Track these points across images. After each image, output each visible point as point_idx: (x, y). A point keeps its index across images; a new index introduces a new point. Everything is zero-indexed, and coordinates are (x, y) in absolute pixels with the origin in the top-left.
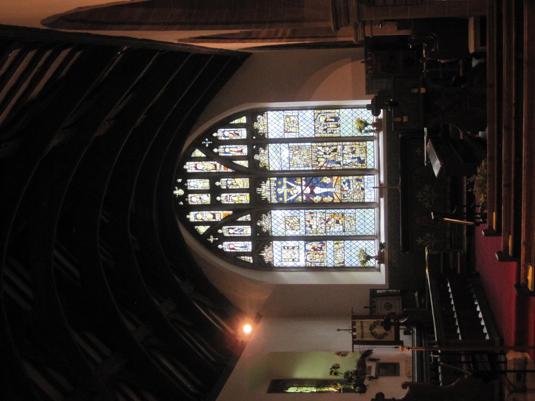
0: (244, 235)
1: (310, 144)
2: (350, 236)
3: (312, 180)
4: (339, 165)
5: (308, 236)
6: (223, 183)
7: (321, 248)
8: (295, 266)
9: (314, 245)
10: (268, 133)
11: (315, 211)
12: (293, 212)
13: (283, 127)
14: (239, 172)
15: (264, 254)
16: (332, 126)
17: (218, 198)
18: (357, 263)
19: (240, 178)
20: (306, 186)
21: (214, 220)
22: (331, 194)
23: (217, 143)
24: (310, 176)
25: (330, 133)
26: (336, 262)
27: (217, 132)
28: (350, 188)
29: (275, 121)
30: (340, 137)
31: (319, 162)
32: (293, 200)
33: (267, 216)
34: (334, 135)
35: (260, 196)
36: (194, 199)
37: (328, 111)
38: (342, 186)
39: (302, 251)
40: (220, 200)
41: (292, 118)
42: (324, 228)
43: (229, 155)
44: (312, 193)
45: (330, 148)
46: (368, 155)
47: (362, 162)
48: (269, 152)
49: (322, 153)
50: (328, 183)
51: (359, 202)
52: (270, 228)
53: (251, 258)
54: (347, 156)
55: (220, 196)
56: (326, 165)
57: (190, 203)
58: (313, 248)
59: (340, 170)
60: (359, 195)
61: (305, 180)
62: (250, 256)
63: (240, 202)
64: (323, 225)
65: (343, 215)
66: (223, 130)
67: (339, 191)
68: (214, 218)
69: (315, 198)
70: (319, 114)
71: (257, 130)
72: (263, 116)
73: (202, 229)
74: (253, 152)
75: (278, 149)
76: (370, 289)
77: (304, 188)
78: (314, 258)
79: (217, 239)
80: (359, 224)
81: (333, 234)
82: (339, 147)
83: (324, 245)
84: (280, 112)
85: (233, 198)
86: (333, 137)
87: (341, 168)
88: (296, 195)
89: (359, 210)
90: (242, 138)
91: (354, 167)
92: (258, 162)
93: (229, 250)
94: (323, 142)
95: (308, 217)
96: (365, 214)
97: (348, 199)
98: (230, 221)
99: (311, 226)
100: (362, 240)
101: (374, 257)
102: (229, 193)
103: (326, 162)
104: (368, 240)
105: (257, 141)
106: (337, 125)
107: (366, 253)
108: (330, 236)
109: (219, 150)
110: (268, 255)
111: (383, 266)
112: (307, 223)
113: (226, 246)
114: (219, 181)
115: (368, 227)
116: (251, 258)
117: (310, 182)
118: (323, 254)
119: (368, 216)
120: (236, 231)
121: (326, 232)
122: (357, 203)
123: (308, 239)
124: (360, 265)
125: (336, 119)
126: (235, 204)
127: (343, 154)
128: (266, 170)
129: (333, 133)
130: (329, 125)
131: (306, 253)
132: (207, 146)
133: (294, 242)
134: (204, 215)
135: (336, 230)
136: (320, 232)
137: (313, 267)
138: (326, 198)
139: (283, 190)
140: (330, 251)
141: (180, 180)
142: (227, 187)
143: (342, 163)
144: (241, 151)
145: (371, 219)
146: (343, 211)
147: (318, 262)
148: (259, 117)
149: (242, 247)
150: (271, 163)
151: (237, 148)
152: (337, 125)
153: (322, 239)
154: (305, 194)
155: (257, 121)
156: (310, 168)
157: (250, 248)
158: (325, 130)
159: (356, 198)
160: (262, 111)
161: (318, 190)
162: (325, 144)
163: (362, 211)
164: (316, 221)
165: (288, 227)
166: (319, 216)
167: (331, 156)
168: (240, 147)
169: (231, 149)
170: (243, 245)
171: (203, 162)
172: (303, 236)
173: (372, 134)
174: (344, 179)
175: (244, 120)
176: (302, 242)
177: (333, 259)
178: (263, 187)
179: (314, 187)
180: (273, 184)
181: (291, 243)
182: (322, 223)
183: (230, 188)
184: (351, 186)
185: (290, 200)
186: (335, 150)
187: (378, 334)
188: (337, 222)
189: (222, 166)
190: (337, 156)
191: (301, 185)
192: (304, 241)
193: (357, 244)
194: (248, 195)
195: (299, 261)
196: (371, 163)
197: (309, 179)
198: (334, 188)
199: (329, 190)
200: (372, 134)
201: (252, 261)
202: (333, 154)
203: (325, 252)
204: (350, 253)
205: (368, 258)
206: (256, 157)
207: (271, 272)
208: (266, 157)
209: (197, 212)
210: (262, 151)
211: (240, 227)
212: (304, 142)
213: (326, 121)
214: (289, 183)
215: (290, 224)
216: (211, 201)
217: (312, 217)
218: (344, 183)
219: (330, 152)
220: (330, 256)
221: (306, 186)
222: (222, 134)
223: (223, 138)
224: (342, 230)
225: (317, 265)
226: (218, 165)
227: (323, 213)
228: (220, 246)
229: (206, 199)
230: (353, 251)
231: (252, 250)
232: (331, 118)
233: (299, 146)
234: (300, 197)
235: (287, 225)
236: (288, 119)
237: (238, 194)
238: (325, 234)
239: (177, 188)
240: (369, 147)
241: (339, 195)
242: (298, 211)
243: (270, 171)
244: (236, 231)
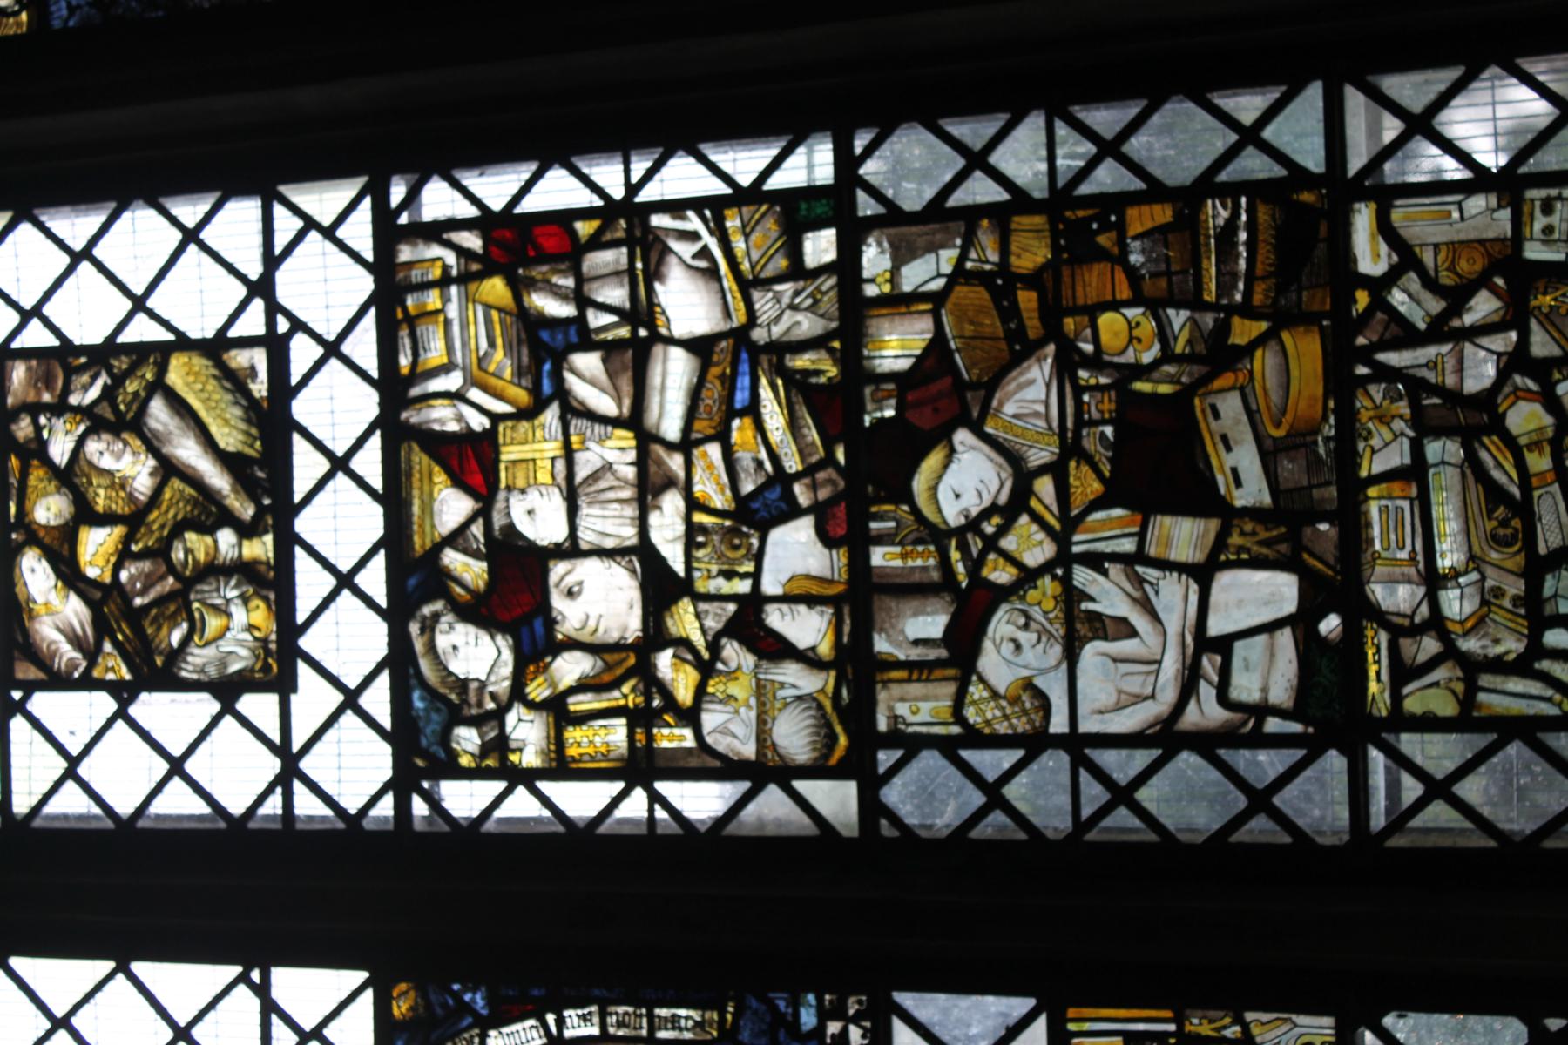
11: (610, 175)
64: (795, 550)
65: (1306, 214)
81: (1043, 794)
99: (517, 592)
146: (1300, 133)
166: (687, 305)
182: (757, 513)
215: (96, 546)
217: (542, 349)
224: (1267, 673)
227: (798, 212)
238: (836, 800)
242: (237, 225)
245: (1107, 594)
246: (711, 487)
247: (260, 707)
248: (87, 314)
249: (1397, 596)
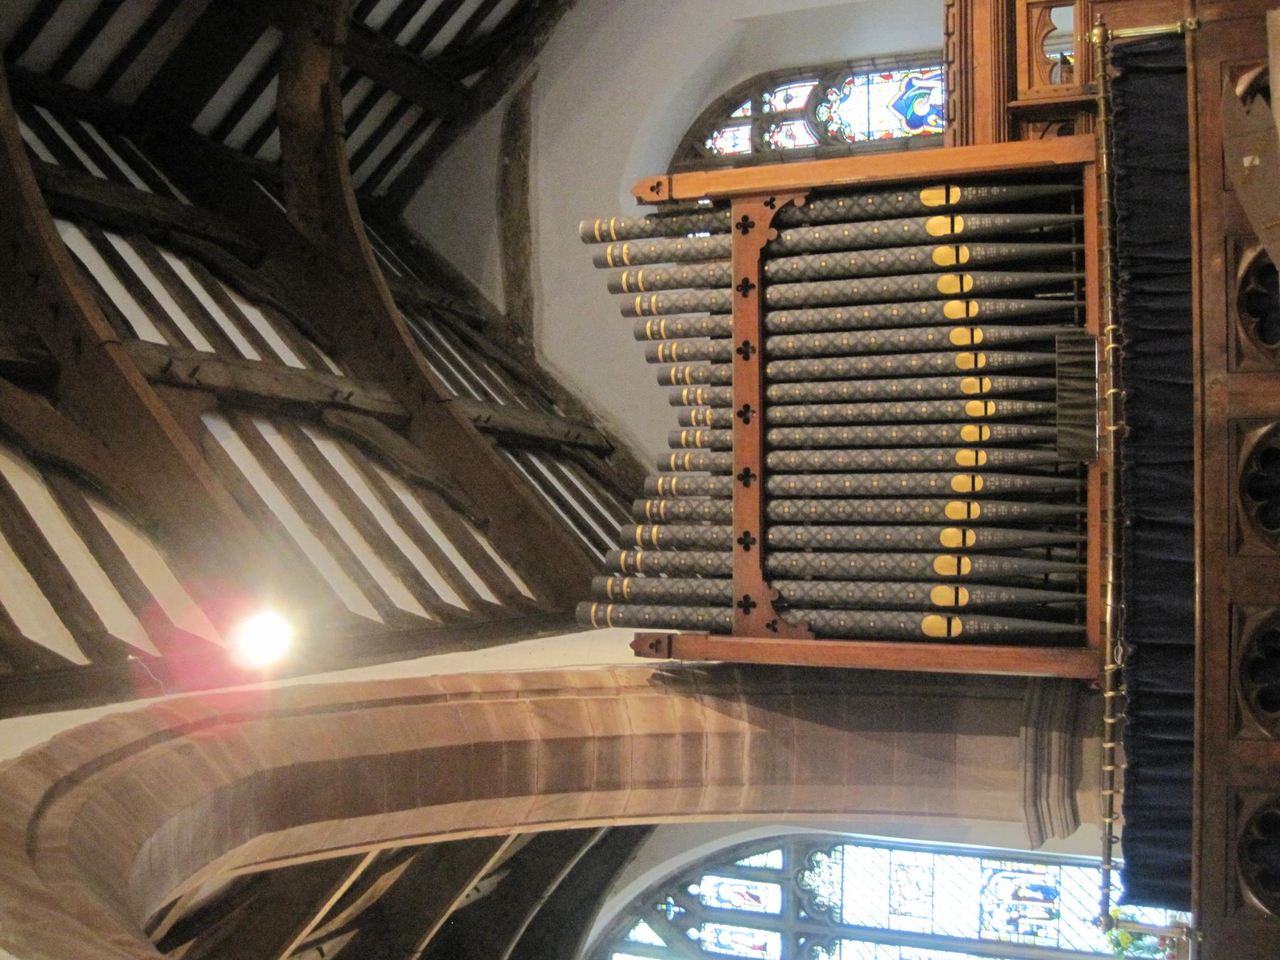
23: (699, 913)
25: (1025, 933)
34: (1039, 941)
37: (1023, 866)
70: (995, 872)
71: (812, 894)
72: (829, 856)
106: (1049, 912)
125: (1049, 894)
129: (1035, 934)
130: (1025, 908)
144: (764, 948)
152: (1049, 912)
155: (811, 869)
169: (735, 937)
213: (1016, 896)
222: (710, 889)
232: (1034, 888)
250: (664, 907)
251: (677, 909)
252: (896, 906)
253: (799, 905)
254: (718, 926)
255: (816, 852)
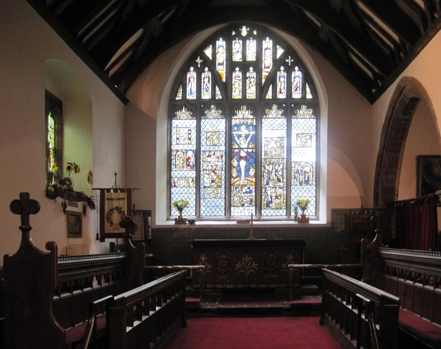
0: (202, 92)
1: (285, 157)
2: (200, 193)
3: (253, 158)
4: (265, 184)
5: (200, 153)
6: (252, 74)
7: (188, 165)
8: (173, 140)
9: (192, 158)
10: (297, 118)
12: (223, 139)
13: (301, 133)
14: (262, 89)
15: (184, 111)
16: (301, 178)
17: (237, 69)
18: (175, 199)
19: (256, 91)
20: (247, 153)
21: (217, 64)
22: (239, 176)
23: (289, 70)
24: (256, 156)
25: (295, 175)
26: (176, 179)
27: (299, 70)
28: (244, 193)
29: (307, 125)
30: (291, 185)
31: (268, 165)
32: (235, 140)
33: (220, 115)
34: (293, 180)
35: (239, 109)
36: (237, 46)
37: (314, 174)
38: (246, 186)
39: (186, 147)
40: (235, 71)
41: (309, 141)
42: (208, 168)
43: (278, 81)
44: (241, 158)
45: (281, 175)
46: (274, 210)
47: (268, 205)
48: (279, 118)
49: (276, 168)
50: (250, 173)
51: (231, 202)
52: (209, 117)
53: (180, 98)
54: (274, 191)
55: (239, 71)
56: (266, 171)
57: (233, 42)
58: (189, 158)
59: (261, 185)
60: (237, 202)
61: (252, 152)
62: (182, 97)
63: (233, 90)
64: (210, 168)
65: (220, 186)
66: (301, 76)
67: (241, 184)
68: (219, 64)
69: (235, 160)
70: (312, 166)
71: (300, 108)
72: (312, 114)
73: (208, 52)
74: (280, 103)
75: (282, 128)
76: (151, 211)
77: (246, 150)
78: (179, 159)
79: (199, 66)
80: (211, 201)
81: (202, 177)
82: (281, 184)
83: (191, 168)
84: (315, 131)
85: (237, 83)
86: (291, 178)
87: (263, 186)
88: (239, 143)
89: (224, 201)
90: (293, 94)
91: (263, 197)
92: (271, 109)
93: (188, 78)
94: (287, 169)
95: (218, 154)
96: (220, 207)
97: (234, 192)
98: (216, 79)
99: (209, 156)
100: (196, 204)
101: (181, 215)
102: (242, 79)
103: (268, 171)
104: (196, 209)
105: (289, 108)
106: (302, 182)
107: (185, 207)
108: (200, 174)
109: (282, 72)
110: (183, 115)
111: (173, 223)
112: (212, 153)
113: (192, 74)
114: (253, 70)
115: (208, 209)
116: (180, 98)
117: (250, 156)
118: (183, 167)
119: (218, 210)
120: (206, 85)
121: (204, 170)
122: (231, 200)
123: (197, 153)
124: (173, 201)
125: (307, 182)
126: (232, 85)
127: (276, 188)
128: (263, 116)
129: (295, 178)
130: (302, 175)
131: (184, 151)
132: (287, 61)
133: (195, 140)
134: (222, 55)
135: (206, 180)
136: (204, 165)
137: (171, 157)
138: (235, 171)
139: (244, 131)
140: (186, 173)
141: (255, 33)
142: (248, 78)
143: (267, 186)
145: (216, 213)
146: (223, 186)
147: (176, 162)
148: (311, 110)
149: (191, 90)
150: (269, 120)
151: (284, 89)
152: (302, 182)
153: (197, 167)
154: (240, 151)
155: (308, 108)
156: (263, 157)
157: (189, 97)
158: (298, 171)
159: (235, 199)
160: (317, 114)
161: (243, 163)
162: (285, 171)
163: (223, 204)
164: (214, 161)
165: (209, 134)
166: (220, 164)
167: (274, 176)
168: (284, 91)
169: (283, 83)
170: (193, 91)
171: (272, 56)
172: (200, 148)
173: (293, 214)
174: (253, 188)
175: (309, 96)
176: (194, 148)
177: (179, 176)
178: (247, 112)
179: (245, 160)
180: (250, 122)
181: (194, 136)
182: (212, 166)
183: (247, 80)
184: (245, 195)
185: (234, 137)
186: (279, 180)
187: (112, 216)
188: (213, 181)
189: (267, 74)
190: (274, 182)
191: (248, 148)
192: (196, 150)
193: (192, 199)
194: (240, 97)
195: (177, 144)
196: (266, 213)
197: (254, 155)
198: (244, 180)
199: (243, 174)
200: (293, 214)
201: (177, 99)
202: (275, 178)
203: (185, 169)
204: (184, 192)
205: (180, 209)
206: (275, 107)
207: (167, 116)
208: (274, 115)
209: (225, 48)
210: (280, 112)
211: (210, 88)
212: (287, 152)
213: (306, 172)
214: (250, 137)
215: (212, 136)
216: (235, 62)
217: (218, 158)
218: (249, 188)
219: (278, 175)
220: (181, 173)
221: (247, 153)
222: (297, 74)
223: (293, 76)
224: (206, 185)
225: (173, 161)
226: (269, 70)
227: (222, 168)
228: (192, 69)
229: (237, 58)
230: (186, 196)
231: (188, 100)
232: (308, 177)
233: (283, 147)
234: (237, 147)
235: (211, 133)
236: (308, 137)
237: (241, 87)
238: (202, 169)
239: (248, 29)
240: (281, 211)
241: (238, 183)
242: (223, 144)
243: (262, 119)
244: (206, 85)
245: (209, 179)
246: (213, 164)
247: (205, 144)
248: (221, 136)
249: (208, 189)
250: (290, 58)
251: (290, 63)
252: (299, 135)
253: (295, 105)
254: (286, 77)
255: (313, 109)
